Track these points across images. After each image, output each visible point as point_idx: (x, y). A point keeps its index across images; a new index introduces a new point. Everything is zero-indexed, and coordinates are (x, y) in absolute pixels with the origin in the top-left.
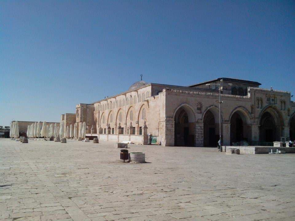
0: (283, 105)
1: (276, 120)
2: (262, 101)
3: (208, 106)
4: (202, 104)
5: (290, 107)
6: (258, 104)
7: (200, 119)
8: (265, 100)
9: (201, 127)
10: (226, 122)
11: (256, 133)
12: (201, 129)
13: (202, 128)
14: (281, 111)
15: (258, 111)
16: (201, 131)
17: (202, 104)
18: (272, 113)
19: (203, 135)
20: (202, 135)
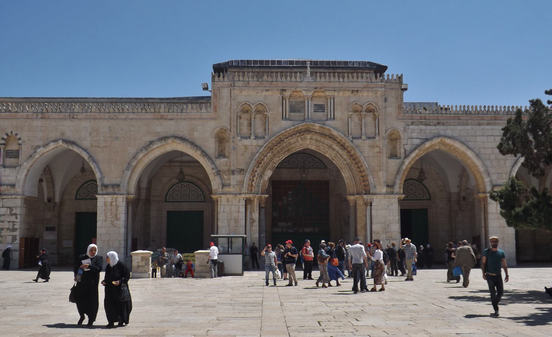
0: (369, 118)
1: (346, 174)
2: (261, 110)
3: (40, 143)
4: (20, 139)
5: (400, 126)
6: (250, 125)
7: (7, 185)
8: (275, 111)
9: (11, 208)
10: (110, 190)
11: (237, 221)
12: (11, 214)
13: (14, 212)
14: (356, 142)
15: (246, 147)
16: (9, 222)
17: (20, 139)
18: (329, 154)
19: (17, 233)
20: (13, 233)
